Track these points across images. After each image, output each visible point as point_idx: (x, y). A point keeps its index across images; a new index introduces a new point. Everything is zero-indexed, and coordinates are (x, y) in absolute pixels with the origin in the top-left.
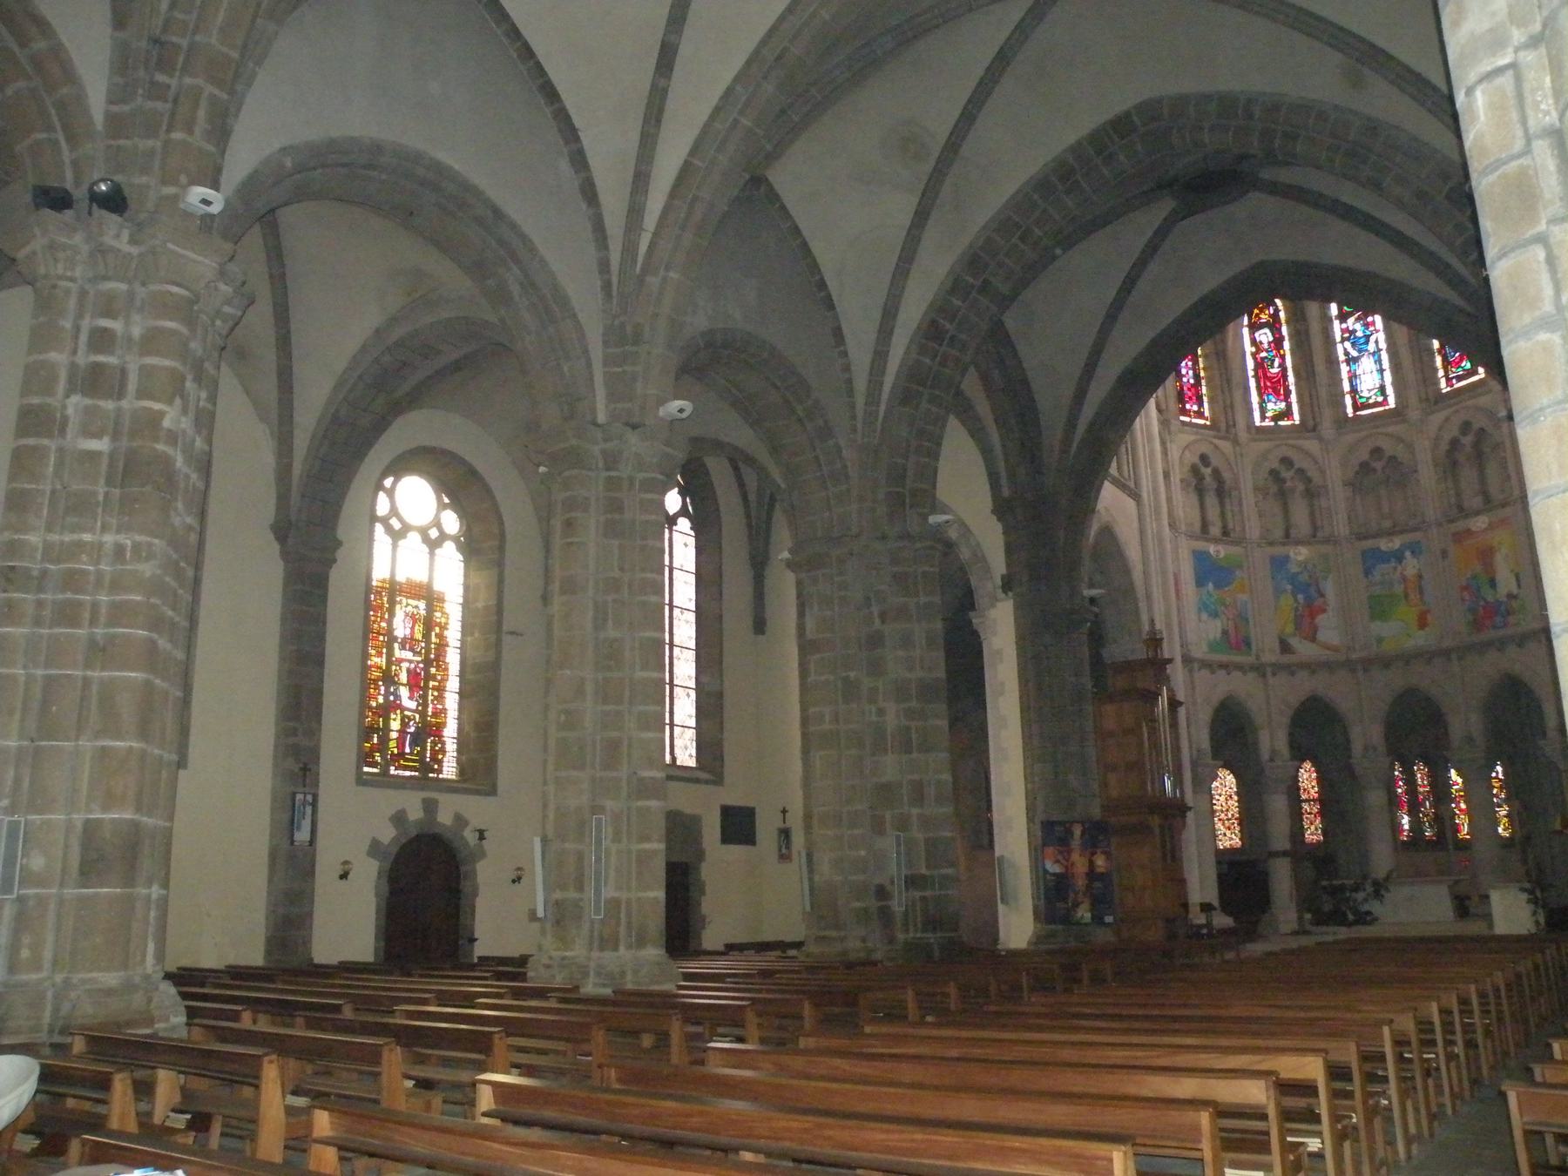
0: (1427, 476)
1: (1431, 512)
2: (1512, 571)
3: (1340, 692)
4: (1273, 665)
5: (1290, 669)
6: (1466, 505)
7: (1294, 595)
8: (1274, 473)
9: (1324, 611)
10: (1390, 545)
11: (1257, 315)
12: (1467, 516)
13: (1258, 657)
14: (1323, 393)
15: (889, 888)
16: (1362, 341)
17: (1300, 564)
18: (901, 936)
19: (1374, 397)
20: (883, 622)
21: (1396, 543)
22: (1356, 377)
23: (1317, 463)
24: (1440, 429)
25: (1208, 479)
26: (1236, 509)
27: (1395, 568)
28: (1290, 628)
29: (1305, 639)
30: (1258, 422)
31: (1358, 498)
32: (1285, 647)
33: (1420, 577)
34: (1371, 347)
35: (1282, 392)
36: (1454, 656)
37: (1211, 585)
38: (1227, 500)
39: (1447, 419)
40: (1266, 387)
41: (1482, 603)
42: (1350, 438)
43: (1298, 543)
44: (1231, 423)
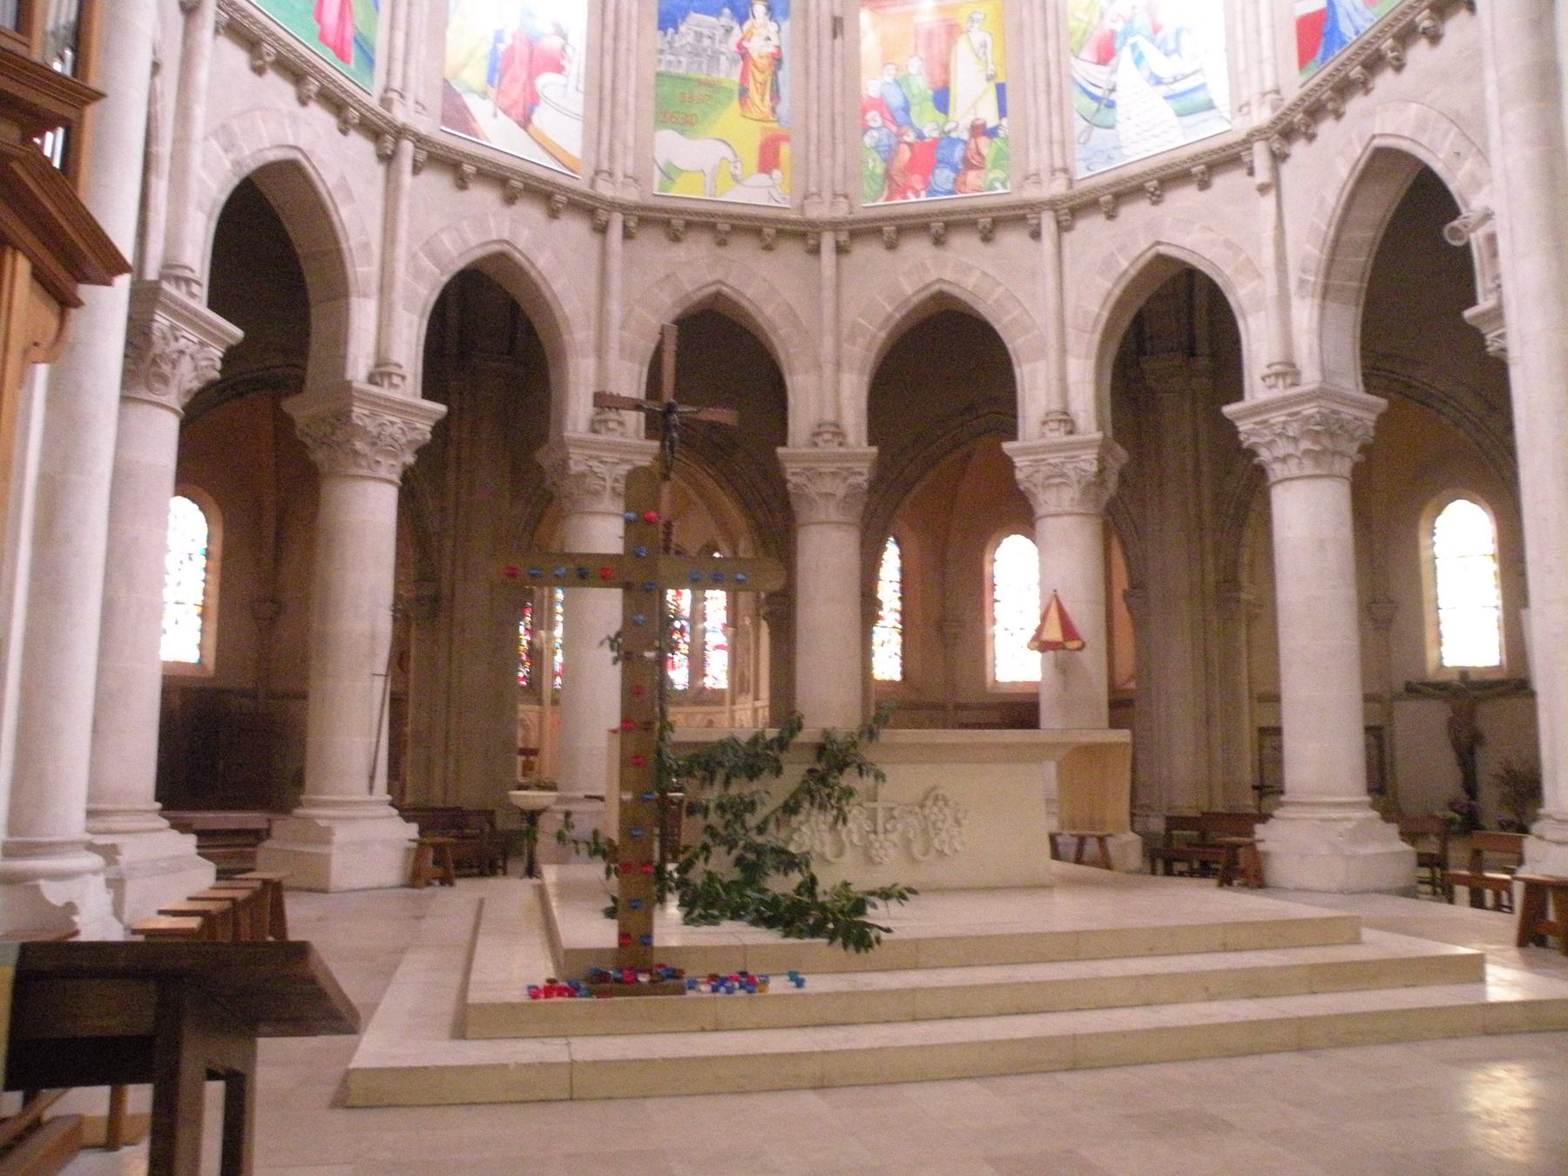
2: (989, 78)
4: (419, 140)
13: (386, 102)
27: (729, 31)
29: (506, 112)
33: (777, 60)
36: (828, 242)
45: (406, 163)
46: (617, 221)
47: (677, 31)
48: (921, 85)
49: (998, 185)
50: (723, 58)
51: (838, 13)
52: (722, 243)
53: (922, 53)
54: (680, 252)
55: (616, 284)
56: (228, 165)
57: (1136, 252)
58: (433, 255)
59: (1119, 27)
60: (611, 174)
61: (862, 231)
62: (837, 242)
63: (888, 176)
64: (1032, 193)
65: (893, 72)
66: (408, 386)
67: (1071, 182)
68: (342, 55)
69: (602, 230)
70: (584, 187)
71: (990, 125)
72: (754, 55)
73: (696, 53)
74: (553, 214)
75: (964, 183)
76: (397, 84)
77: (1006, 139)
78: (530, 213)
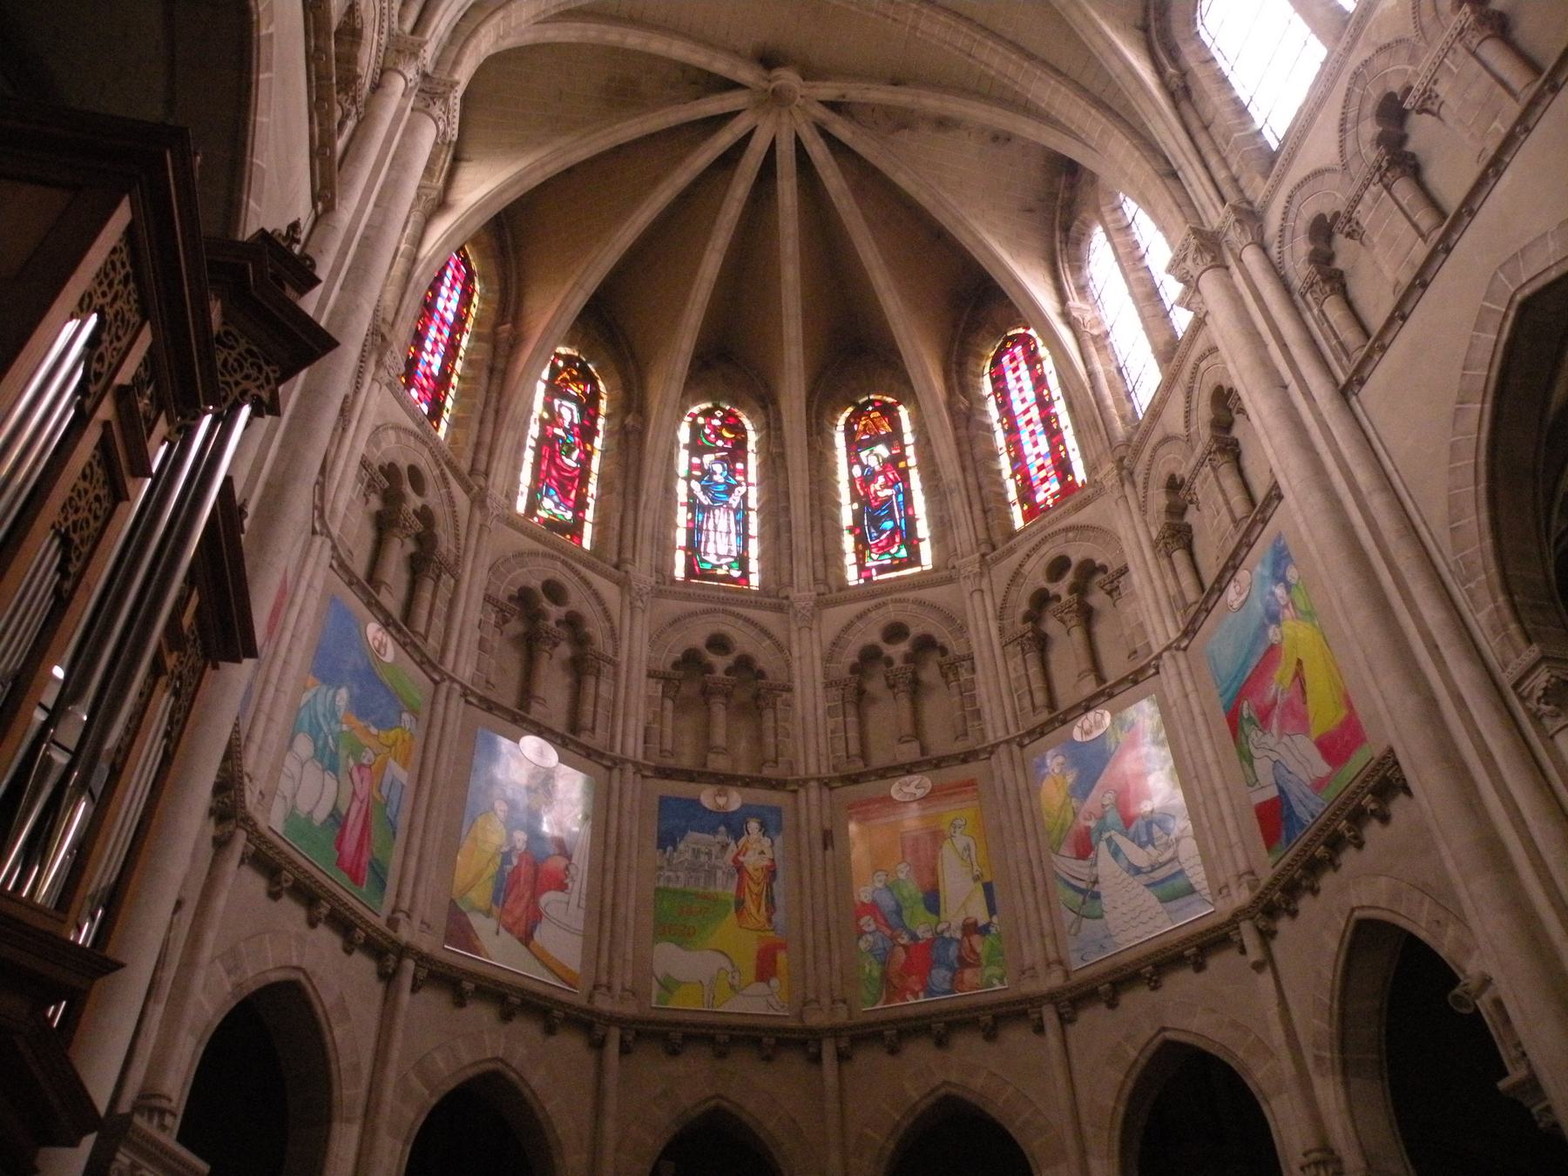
2: (976, 879)
4: (422, 959)
8: (524, 597)
10: (721, 801)
11: (564, 380)
13: (392, 923)
14: (647, 519)
16: (721, 488)
19: (725, 568)
21: (734, 800)
22: (700, 530)
23: (609, 618)
24: (849, 626)
26: (441, 606)
27: (725, 847)
28: (480, 895)
29: (509, 930)
31: (669, 704)
33: (771, 873)
34: (735, 500)
35: (573, 496)
36: (828, 1051)
37: (343, 694)
38: (428, 585)
39: (860, 617)
40: (549, 475)
41: (905, 940)
42: (673, 607)
44: (482, 466)
45: (407, 981)
47: (675, 849)
48: (911, 889)
49: (995, 981)
50: (719, 873)
51: (827, 826)
52: (721, 1055)
53: (909, 859)
55: (611, 1105)
56: (229, 988)
57: (1142, 1039)
59: (1092, 824)
60: (609, 988)
62: (838, 1048)
63: (885, 978)
64: (1030, 987)
65: (883, 878)
67: (1067, 974)
68: (356, 878)
69: (598, 1045)
70: (584, 1003)
71: (982, 922)
72: (750, 869)
73: (693, 869)
74: (550, 1030)
75: (962, 982)
76: (405, 905)
77: (999, 936)
78: (526, 1029)
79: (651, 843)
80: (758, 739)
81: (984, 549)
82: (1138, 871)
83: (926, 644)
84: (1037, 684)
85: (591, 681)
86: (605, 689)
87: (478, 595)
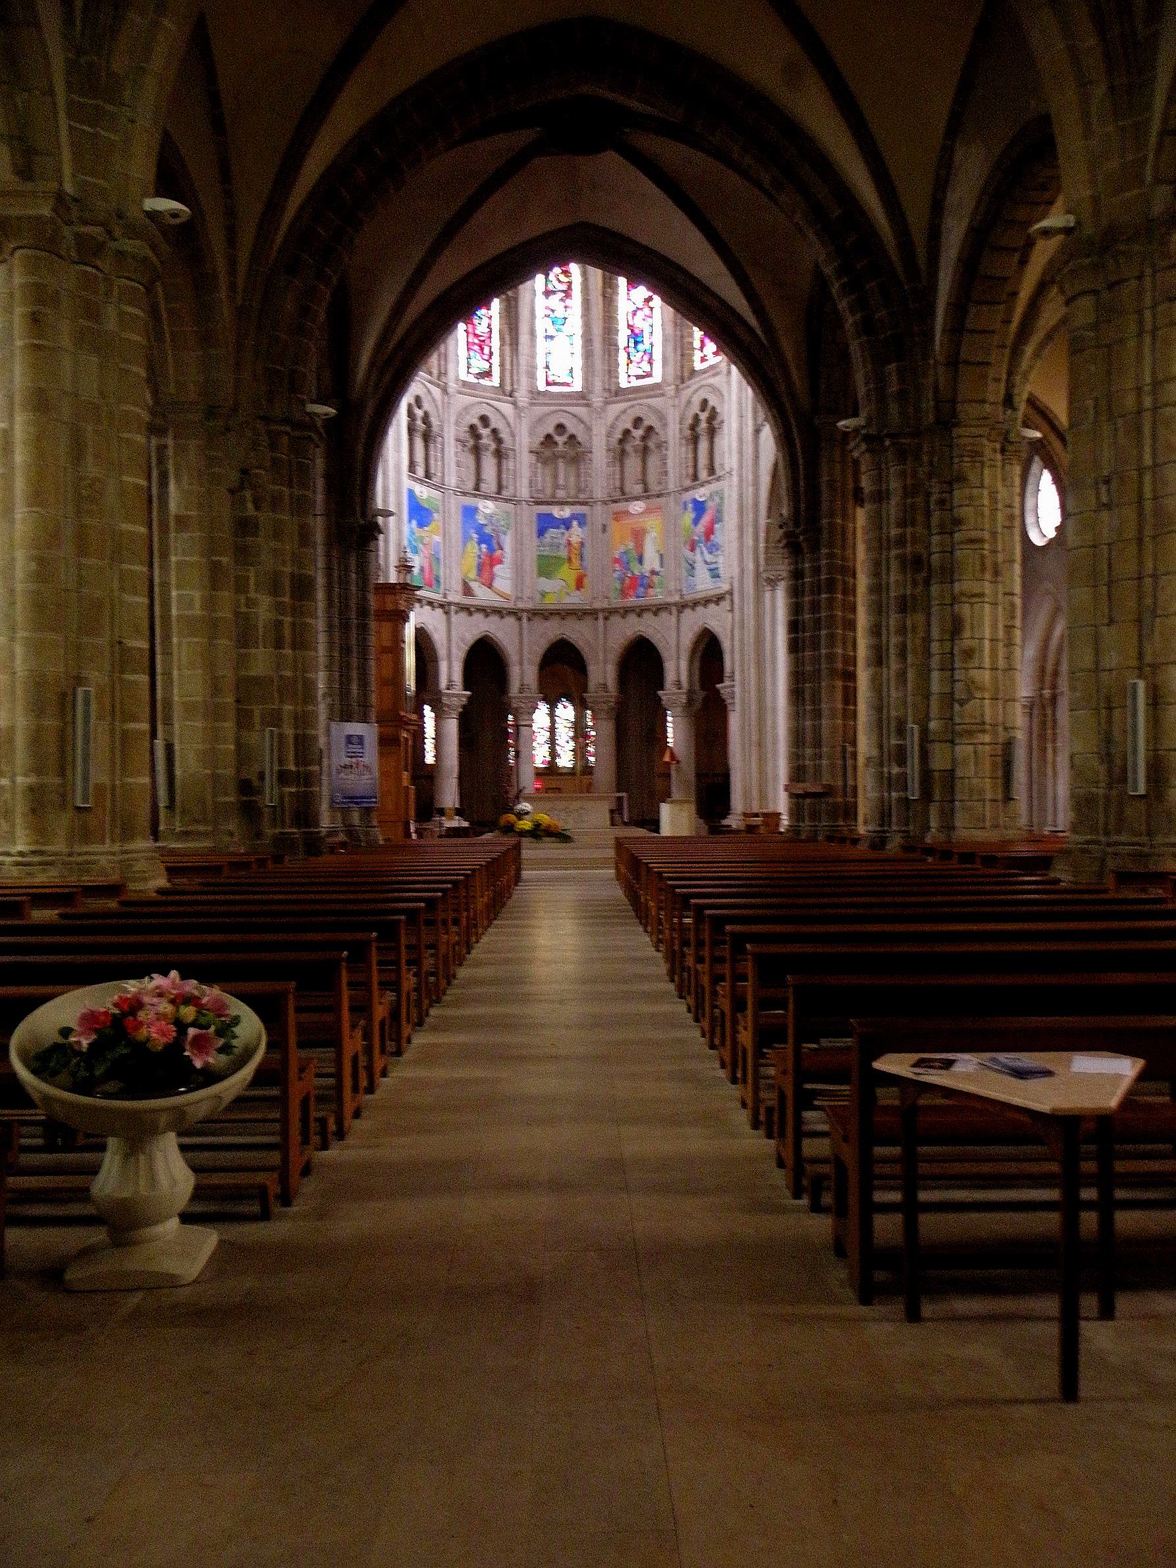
0: (600, 456)
1: (599, 493)
2: (658, 551)
3: (503, 632)
5: (467, 610)
6: (627, 490)
7: (479, 543)
8: (472, 428)
9: (500, 562)
12: (627, 500)
13: (445, 596)
14: (523, 360)
15: (256, 783)
16: (560, 322)
17: (486, 516)
18: (269, 831)
20: (257, 508)
21: (566, 512)
23: (508, 424)
24: (617, 418)
25: (419, 422)
27: (563, 534)
28: (473, 574)
30: (463, 376)
32: (468, 591)
33: (582, 544)
36: (601, 616)
39: (624, 412)
42: (539, 410)
43: (486, 497)
45: (452, 613)
46: (525, 615)
48: (634, 554)
54: (547, 624)
55: (526, 640)
58: (463, 640)
61: (610, 613)
64: (670, 600)
66: (458, 689)
67: (682, 596)
69: (519, 619)
78: (494, 618)
79: (535, 535)
80: (578, 476)
81: (678, 382)
82: (706, 563)
83: (650, 429)
84: (691, 464)
85: (504, 462)
86: (511, 465)
87: (452, 441)
